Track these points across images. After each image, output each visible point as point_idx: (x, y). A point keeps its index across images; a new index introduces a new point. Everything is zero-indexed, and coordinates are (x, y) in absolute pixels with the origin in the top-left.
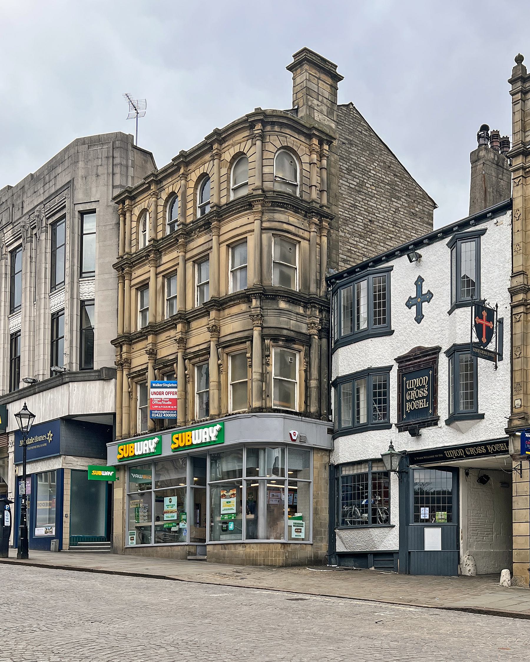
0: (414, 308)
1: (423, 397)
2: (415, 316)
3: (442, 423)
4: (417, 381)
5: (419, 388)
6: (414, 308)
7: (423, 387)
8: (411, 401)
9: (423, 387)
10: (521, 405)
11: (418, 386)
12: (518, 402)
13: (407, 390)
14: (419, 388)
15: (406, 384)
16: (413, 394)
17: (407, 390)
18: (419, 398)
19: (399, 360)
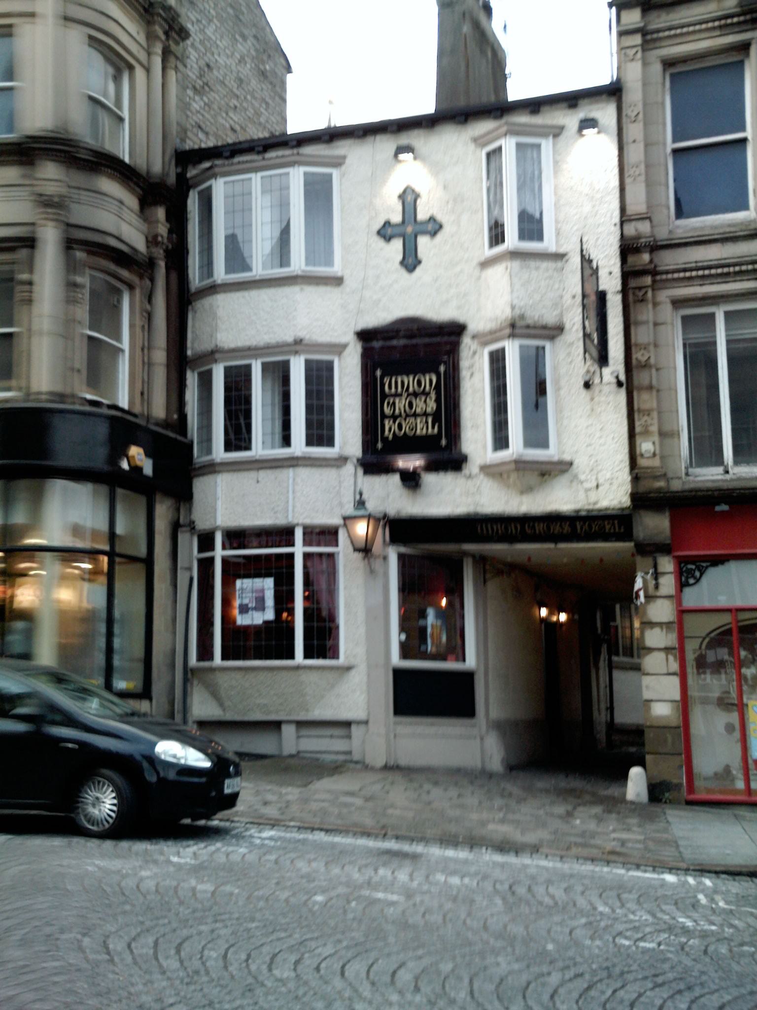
0: (397, 245)
1: (425, 414)
2: (400, 257)
3: (472, 468)
4: (410, 381)
5: (415, 395)
6: (397, 245)
7: (426, 394)
8: (394, 417)
9: (426, 394)
10: (654, 455)
11: (411, 389)
12: (646, 446)
13: (384, 396)
14: (415, 395)
15: (383, 385)
16: (401, 404)
17: (384, 396)
18: (415, 415)
19: (365, 336)
